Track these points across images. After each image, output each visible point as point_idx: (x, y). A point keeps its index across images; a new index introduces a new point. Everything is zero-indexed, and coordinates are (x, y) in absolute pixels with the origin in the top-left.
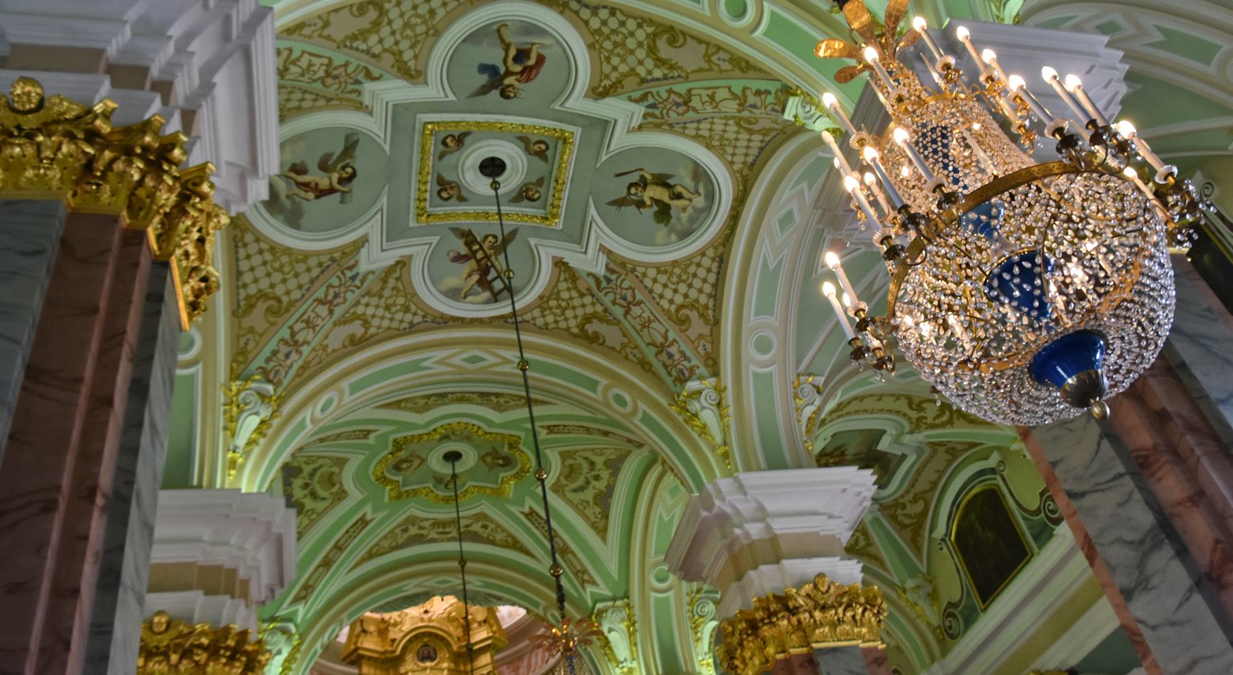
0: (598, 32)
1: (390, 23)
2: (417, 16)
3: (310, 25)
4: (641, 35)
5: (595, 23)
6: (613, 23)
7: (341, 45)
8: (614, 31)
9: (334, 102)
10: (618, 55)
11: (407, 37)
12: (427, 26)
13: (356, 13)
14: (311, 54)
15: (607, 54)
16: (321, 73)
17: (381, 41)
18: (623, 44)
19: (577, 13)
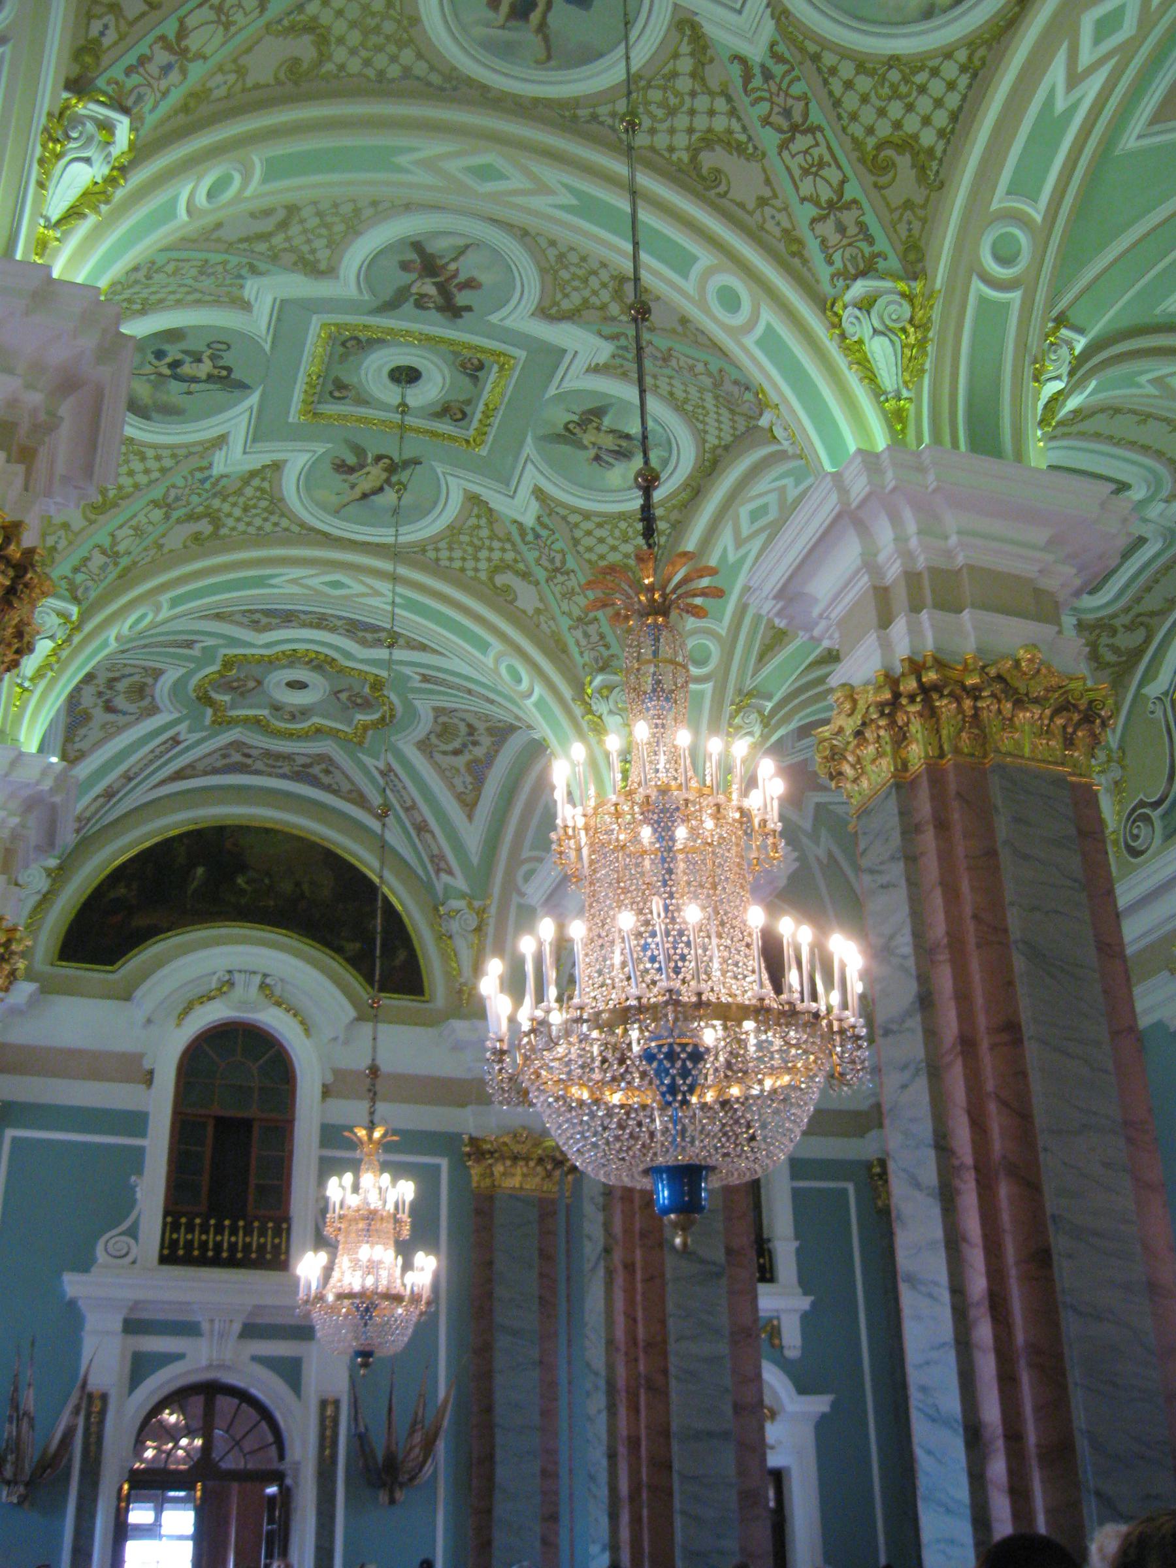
0: (401, 44)
1: (691, 131)
2: (653, 117)
3: (778, 224)
4: (340, 54)
5: (407, 56)
6: (381, 61)
7: (758, 155)
8: (379, 49)
9: (812, 48)
10: (373, 15)
11: (678, 94)
12: (645, 96)
13: (724, 181)
14: (797, 188)
15: (392, 12)
16: (802, 142)
17: (712, 113)
18: (365, 34)
19: (432, 68)
